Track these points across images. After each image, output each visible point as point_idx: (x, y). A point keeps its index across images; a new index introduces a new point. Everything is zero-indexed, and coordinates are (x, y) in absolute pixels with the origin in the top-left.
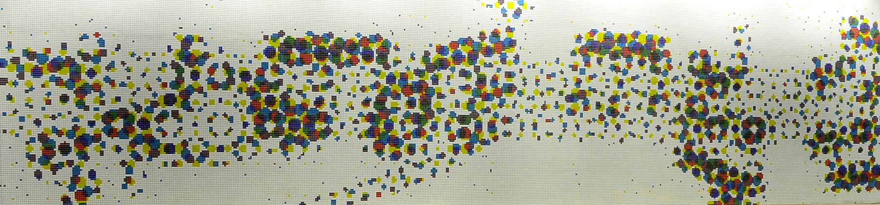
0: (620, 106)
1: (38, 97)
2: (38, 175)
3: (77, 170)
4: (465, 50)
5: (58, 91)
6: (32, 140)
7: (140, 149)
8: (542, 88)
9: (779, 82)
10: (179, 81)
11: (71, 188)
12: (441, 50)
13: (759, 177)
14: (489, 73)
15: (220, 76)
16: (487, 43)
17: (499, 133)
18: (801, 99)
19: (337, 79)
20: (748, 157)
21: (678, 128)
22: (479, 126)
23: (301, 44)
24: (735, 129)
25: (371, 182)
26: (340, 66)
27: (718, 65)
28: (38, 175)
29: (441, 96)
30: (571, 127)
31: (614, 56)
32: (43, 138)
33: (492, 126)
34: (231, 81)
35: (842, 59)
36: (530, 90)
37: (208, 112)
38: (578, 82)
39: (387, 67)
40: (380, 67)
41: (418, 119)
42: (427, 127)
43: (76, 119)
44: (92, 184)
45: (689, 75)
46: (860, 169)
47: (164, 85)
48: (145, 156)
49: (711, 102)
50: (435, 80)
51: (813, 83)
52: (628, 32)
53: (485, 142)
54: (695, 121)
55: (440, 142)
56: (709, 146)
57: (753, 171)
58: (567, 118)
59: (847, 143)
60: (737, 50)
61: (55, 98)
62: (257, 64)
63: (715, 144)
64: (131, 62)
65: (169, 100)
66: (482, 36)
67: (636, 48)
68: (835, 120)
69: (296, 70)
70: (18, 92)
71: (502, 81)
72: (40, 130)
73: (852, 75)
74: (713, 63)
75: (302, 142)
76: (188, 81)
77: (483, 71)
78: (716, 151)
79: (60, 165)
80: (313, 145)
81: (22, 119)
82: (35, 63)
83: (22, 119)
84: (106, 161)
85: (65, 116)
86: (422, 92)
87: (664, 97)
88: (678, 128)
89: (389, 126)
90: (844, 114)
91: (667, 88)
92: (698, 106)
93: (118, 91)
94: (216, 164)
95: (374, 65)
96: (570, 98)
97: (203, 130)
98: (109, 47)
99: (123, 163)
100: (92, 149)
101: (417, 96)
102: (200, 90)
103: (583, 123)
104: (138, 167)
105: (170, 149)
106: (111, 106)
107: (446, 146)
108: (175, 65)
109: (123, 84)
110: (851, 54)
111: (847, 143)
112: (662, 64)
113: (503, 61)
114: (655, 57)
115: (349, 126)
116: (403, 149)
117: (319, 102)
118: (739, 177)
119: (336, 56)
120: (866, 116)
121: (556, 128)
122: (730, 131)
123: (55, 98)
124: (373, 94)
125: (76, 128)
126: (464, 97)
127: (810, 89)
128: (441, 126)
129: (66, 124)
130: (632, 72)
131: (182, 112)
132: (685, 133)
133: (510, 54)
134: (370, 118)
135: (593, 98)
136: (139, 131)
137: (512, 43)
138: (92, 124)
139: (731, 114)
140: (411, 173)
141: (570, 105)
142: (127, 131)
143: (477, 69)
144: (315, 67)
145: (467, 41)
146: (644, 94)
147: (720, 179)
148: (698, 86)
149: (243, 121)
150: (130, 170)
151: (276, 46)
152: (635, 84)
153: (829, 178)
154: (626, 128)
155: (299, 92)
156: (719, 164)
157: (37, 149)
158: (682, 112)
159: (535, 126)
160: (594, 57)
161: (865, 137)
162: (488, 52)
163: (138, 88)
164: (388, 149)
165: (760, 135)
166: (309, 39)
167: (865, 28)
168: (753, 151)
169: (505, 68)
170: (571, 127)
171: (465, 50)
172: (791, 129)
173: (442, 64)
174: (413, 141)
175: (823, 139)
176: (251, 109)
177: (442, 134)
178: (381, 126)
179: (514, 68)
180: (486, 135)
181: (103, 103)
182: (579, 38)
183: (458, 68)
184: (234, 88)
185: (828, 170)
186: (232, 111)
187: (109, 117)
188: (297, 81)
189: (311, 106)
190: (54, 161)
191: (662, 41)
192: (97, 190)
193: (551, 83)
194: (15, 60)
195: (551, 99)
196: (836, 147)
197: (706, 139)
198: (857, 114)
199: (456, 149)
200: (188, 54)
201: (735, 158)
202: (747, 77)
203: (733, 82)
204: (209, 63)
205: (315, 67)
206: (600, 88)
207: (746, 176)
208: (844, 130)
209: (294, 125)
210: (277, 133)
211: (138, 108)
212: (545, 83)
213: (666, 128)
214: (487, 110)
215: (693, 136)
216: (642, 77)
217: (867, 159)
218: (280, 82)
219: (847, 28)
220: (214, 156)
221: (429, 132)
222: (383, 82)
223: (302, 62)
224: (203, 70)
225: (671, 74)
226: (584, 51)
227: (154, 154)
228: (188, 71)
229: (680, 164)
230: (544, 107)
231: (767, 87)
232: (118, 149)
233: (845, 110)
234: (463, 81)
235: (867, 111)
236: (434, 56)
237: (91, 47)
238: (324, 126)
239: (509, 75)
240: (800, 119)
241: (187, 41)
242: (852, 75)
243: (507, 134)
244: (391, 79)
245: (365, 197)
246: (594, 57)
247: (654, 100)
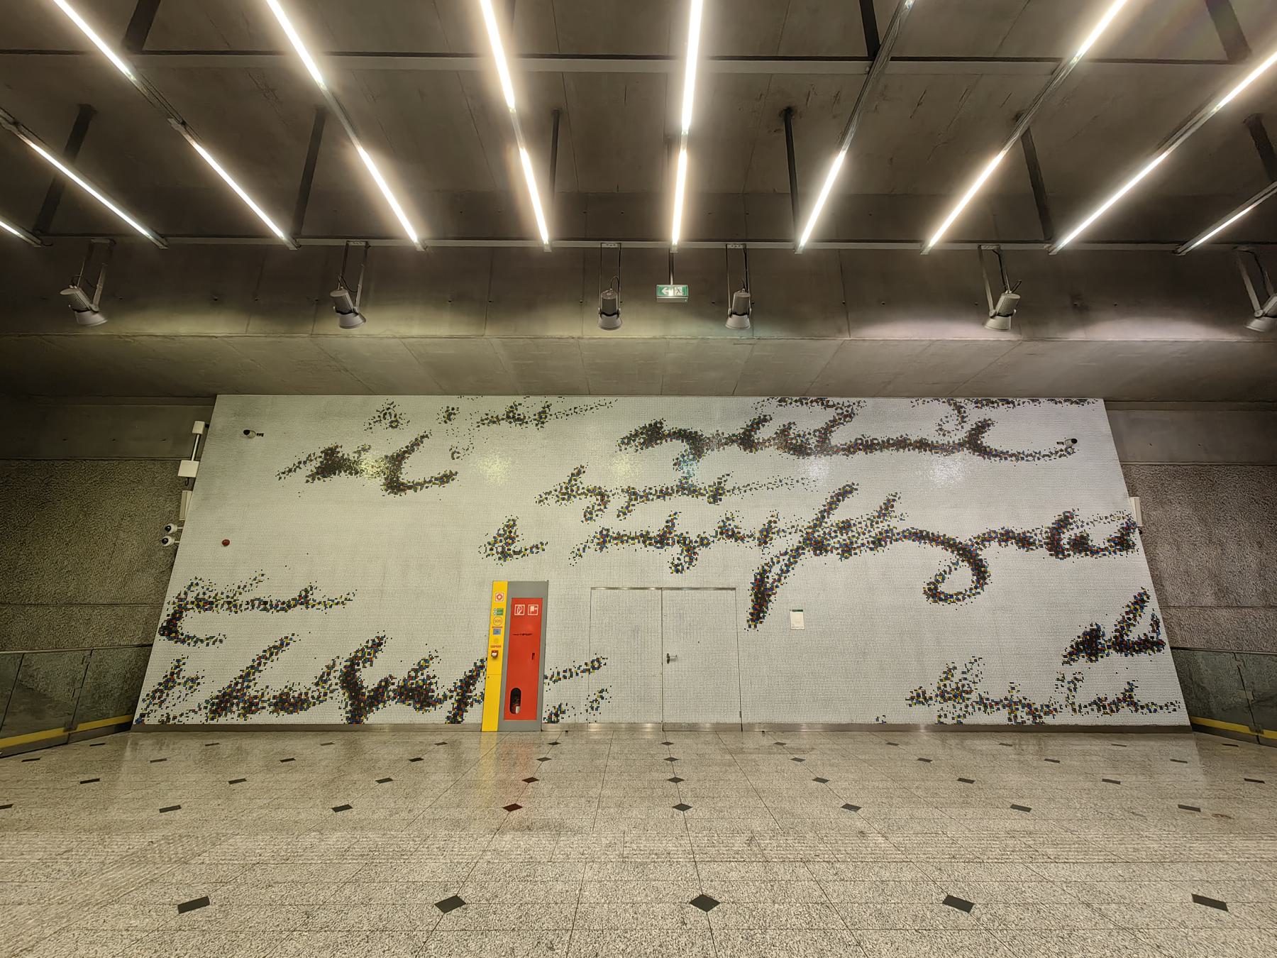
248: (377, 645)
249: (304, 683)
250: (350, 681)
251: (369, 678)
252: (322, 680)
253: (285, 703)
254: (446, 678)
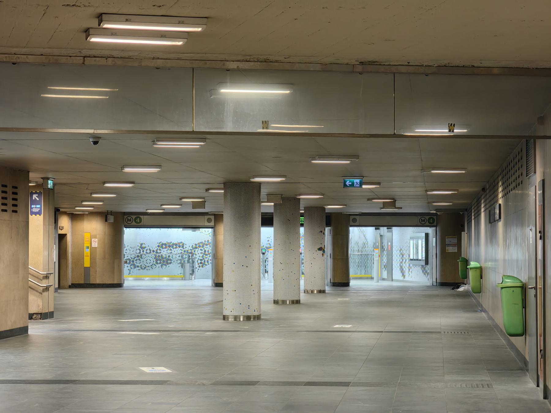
10: (140, 253)
12: (196, 245)
14: (207, 250)
15: (148, 251)
19: (173, 252)
22: (205, 261)
23: (165, 244)
34: (150, 252)
37: (146, 259)
50: (195, 251)
60: (268, 243)
64: (130, 249)
65: (138, 256)
76: (142, 252)
80: (168, 266)
105: (138, 267)
115: (176, 262)
117: (169, 256)
126: (201, 255)
134: (180, 260)
142: (129, 263)
145: (201, 243)
149: (153, 261)
162: (206, 245)
173: (196, 248)
176: (155, 258)
180: (206, 263)
186: (151, 259)
188: (164, 252)
199: (199, 267)
209: (164, 262)
210: (160, 263)
220: (147, 268)
223: (165, 248)
224: (145, 250)
227: (135, 268)
234: (201, 251)
236: (194, 246)
241: (142, 244)
244: (185, 251)
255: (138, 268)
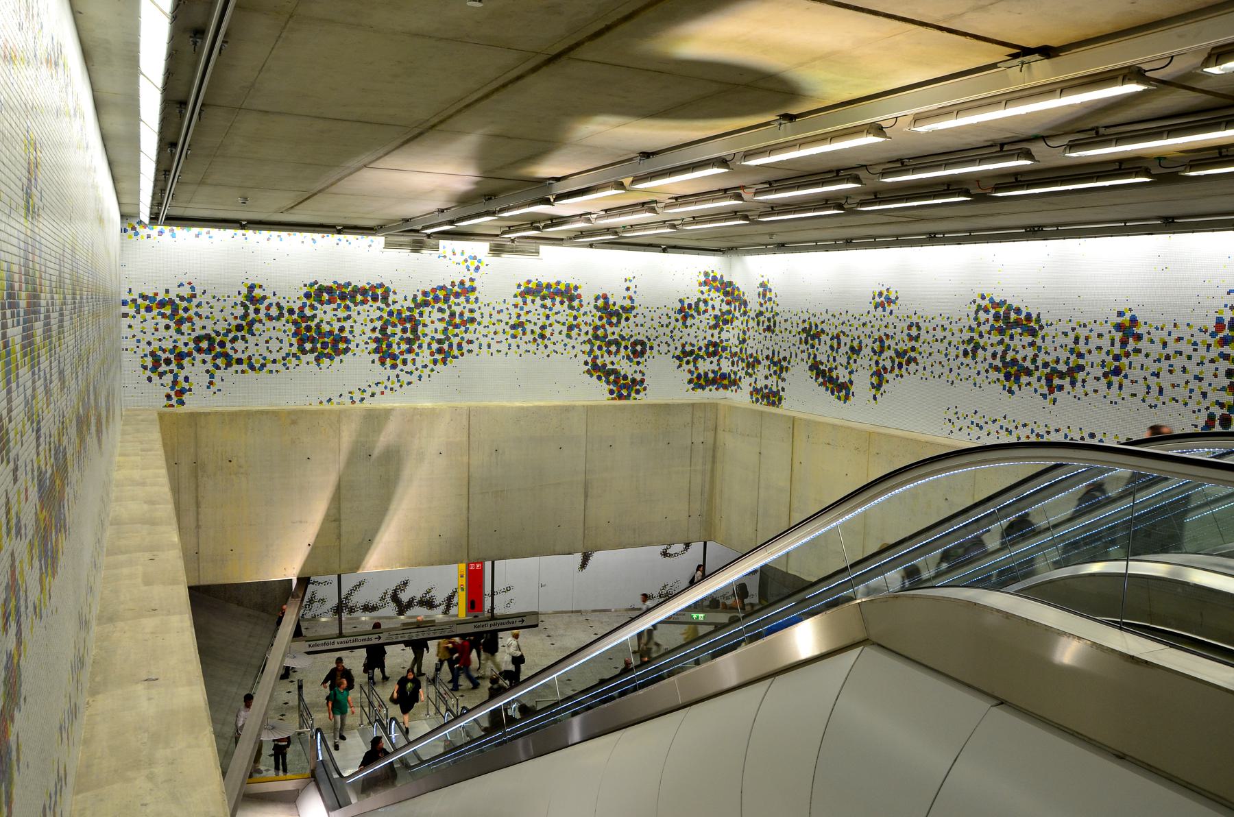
0: (547, 332)
1: (149, 326)
2: (150, 379)
3: (176, 376)
4: (441, 294)
5: (163, 322)
6: (146, 355)
7: (219, 362)
8: (494, 320)
9: (656, 316)
10: (246, 315)
11: (172, 388)
12: (425, 294)
13: (642, 381)
14: (457, 310)
15: (274, 312)
16: (456, 289)
17: (464, 351)
18: (671, 327)
19: (354, 314)
20: (635, 367)
21: (587, 347)
22: (451, 346)
23: (329, 290)
24: (626, 348)
25: (377, 384)
26: (356, 305)
27: (614, 304)
28: (150, 379)
29: (425, 325)
30: (514, 347)
31: (543, 298)
32: (153, 354)
33: (460, 346)
34: (281, 315)
35: (699, 300)
36: (485, 321)
37: (265, 336)
38: (519, 316)
39: (388, 305)
40: (383, 306)
41: (409, 341)
42: (415, 347)
43: (175, 341)
44: (187, 386)
45: (594, 311)
46: (711, 375)
47: (236, 318)
48: (223, 366)
49: (609, 330)
50: (421, 315)
51: (679, 317)
52: (553, 282)
53: (455, 357)
54: (598, 343)
55: (424, 357)
56: (608, 359)
57: (638, 377)
58: (511, 341)
59: (702, 357)
61: (161, 327)
62: (299, 303)
63: (612, 358)
64: (213, 302)
65: (239, 328)
66: (453, 284)
67: (559, 292)
68: (694, 342)
69: (325, 307)
70: (136, 323)
71: (467, 315)
72: (151, 349)
73: (706, 311)
74: (611, 302)
75: (330, 357)
76: (252, 315)
77: (454, 308)
78: (613, 363)
79: (165, 373)
80: (337, 359)
81: (138, 341)
82: (147, 302)
83: (138, 341)
84: (196, 370)
85: (168, 339)
86: (411, 322)
87: (578, 326)
88: (587, 347)
89: (389, 346)
90: (700, 338)
91: (580, 320)
92: (600, 332)
93: (204, 322)
94: (271, 372)
95: (379, 304)
96: (513, 327)
97: (262, 349)
98: (198, 291)
99: (208, 371)
100: (186, 362)
101: (408, 325)
102: (260, 321)
103: (522, 343)
104: (218, 374)
105: (239, 361)
106: (199, 332)
107: (428, 360)
108: (243, 304)
109: (207, 317)
110: (705, 296)
111: (702, 357)
112: (576, 303)
113: (468, 301)
114: (571, 299)
115: (362, 346)
116: (399, 362)
117: (342, 329)
118: (629, 381)
119: (353, 298)
120: (715, 339)
121: (503, 347)
122: (622, 349)
123: (161, 327)
124: (378, 324)
125: (175, 347)
126: (441, 326)
127: (677, 320)
128: (425, 346)
129: (168, 345)
130: (555, 309)
131: (248, 337)
132: (592, 350)
133: (472, 297)
134: (377, 340)
135: (529, 327)
136: (218, 349)
137: (473, 289)
138: (186, 344)
139: (623, 338)
140: (405, 378)
141: (513, 331)
142: (210, 349)
143: (450, 307)
144: (339, 306)
145: (443, 288)
146: (564, 324)
147: (616, 382)
148: (601, 318)
149: (289, 343)
150: (212, 376)
151: (312, 291)
152: (558, 317)
153: (690, 381)
154: (551, 347)
155: (328, 323)
156: (615, 372)
157: (149, 362)
158: (590, 336)
159: (489, 346)
160: (529, 298)
161: (715, 354)
162: (457, 295)
163: (218, 320)
164: (389, 362)
165: (643, 352)
166: (334, 286)
167: (715, 279)
168: (638, 363)
169: (469, 306)
170: (514, 347)
171: (441, 294)
172: (664, 348)
173: (426, 303)
174: (406, 356)
175: (686, 355)
176: (295, 334)
177: (425, 351)
178: (384, 346)
179: (475, 306)
180: (455, 352)
181: (194, 330)
182: (519, 286)
183: (437, 306)
184: (283, 320)
185: (689, 376)
186: (282, 336)
187: (198, 340)
188: (327, 315)
189: (336, 332)
190: (161, 370)
191: (576, 288)
192: (190, 390)
193: (500, 316)
194: (134, 301)
195: (500, 327)
196: (695, 360)
197: (606, 355)
198: (709, 338)
199: (435, 362)
200: (252, 297)
201: (626, 368)
202: (634, 312)
203: (624, 316)
204: (266, 303)
205: (339, 306)
206: (534, 319)
207: (634, 380)
208: (700, 349)
209: (324, 345)
210: (312, 351)
211: (218, 334)
212: (496, 317)
213: (579, 347)
214: (456, 335)
215: (597, 353)
216: (562, 311)
217: (716, 368)
218: (315, 316)
219: (702, 279)
220: (270, 366)
221: (417, 350)
222: (385, 316)
223: (329, 302)
224: (262, 307)
225: (582, 310)
226: (523, 294)
227: (228, 365)
228: (252, 308)
229: (588, 372)
230: (495, 333)
231: (648, 319)
232: (204, 362)
233: (701, 335)
234: (440, 315)
235: (716, 335)
236: (420, 298)
237: (186, 292)
238: (345, 346)
239: (471, 311)
240: (670, 341)
241: (251, 288)
242: (706, 311)
243: (470, 351)
244: (391, 314)
245: (373, 395)
246: (529, 298)
247: (570, 328)
248: (405, 583)
249: (374, 599)
250: (395, 598)
251: (404, 597)
252: (382, 599)
253: (367, 608)
254: (440, 597)
255: (239, 368)
